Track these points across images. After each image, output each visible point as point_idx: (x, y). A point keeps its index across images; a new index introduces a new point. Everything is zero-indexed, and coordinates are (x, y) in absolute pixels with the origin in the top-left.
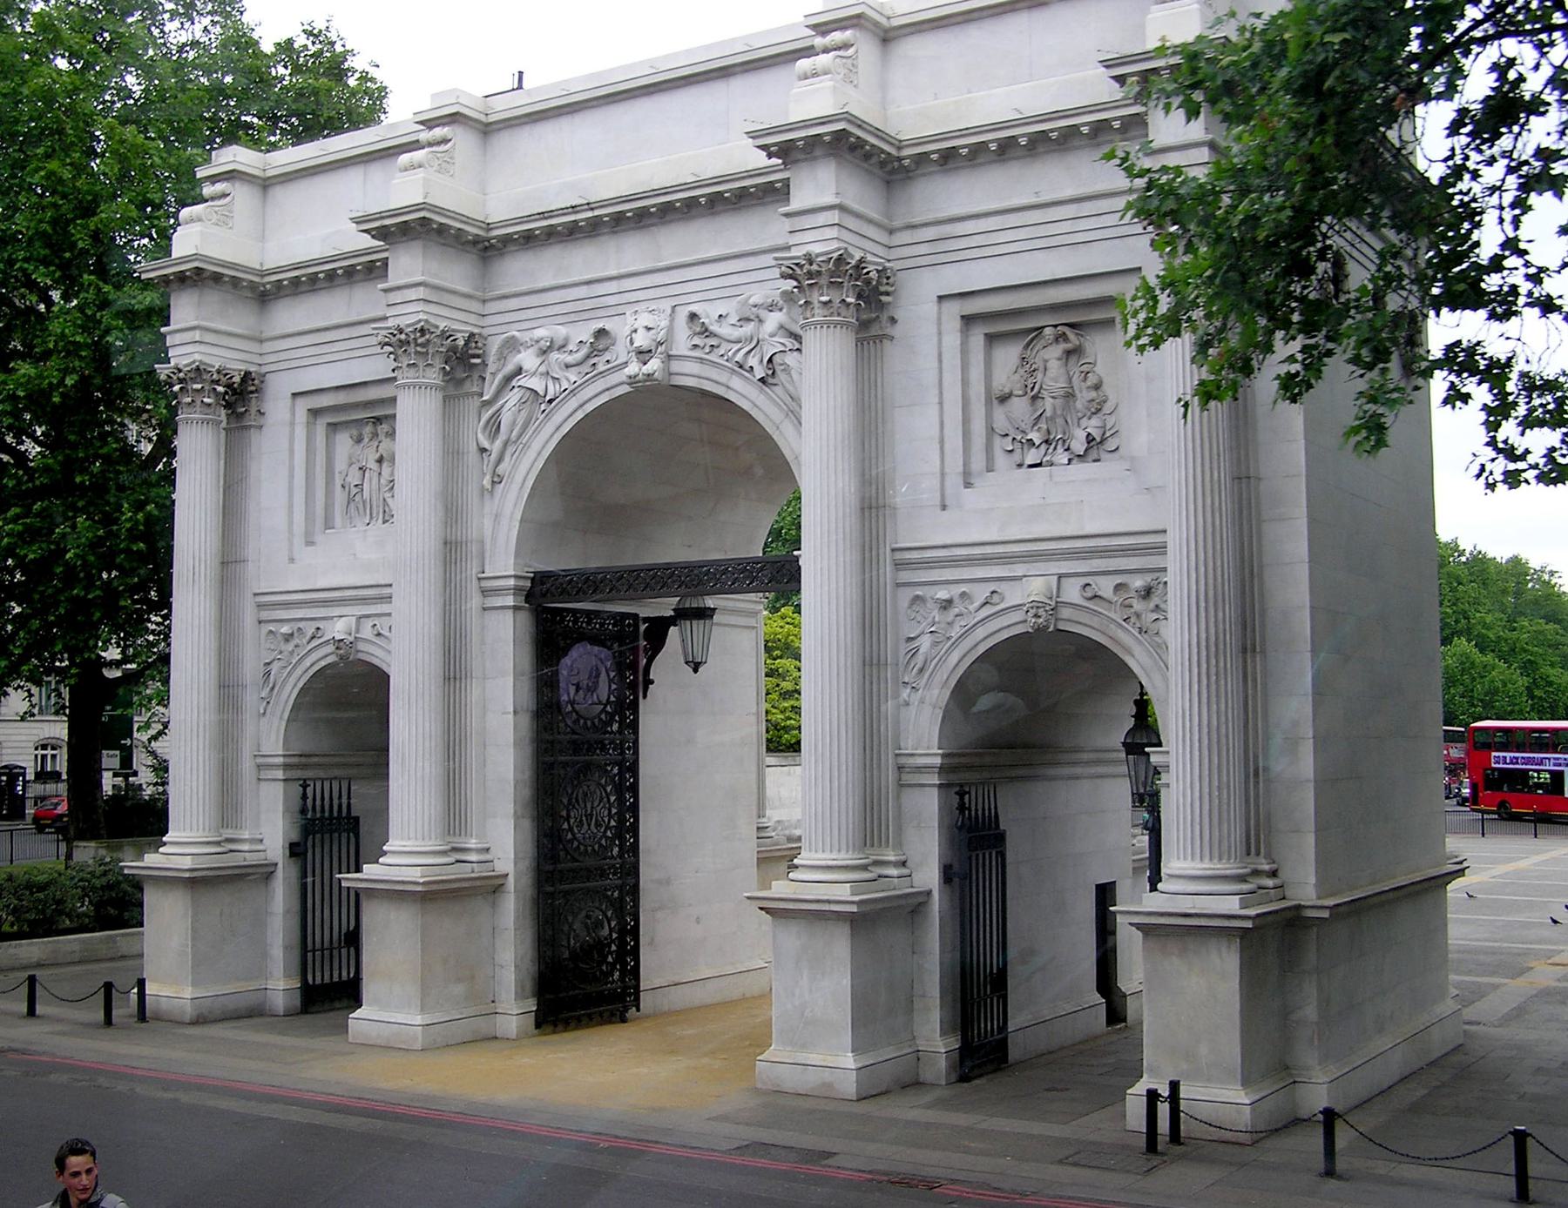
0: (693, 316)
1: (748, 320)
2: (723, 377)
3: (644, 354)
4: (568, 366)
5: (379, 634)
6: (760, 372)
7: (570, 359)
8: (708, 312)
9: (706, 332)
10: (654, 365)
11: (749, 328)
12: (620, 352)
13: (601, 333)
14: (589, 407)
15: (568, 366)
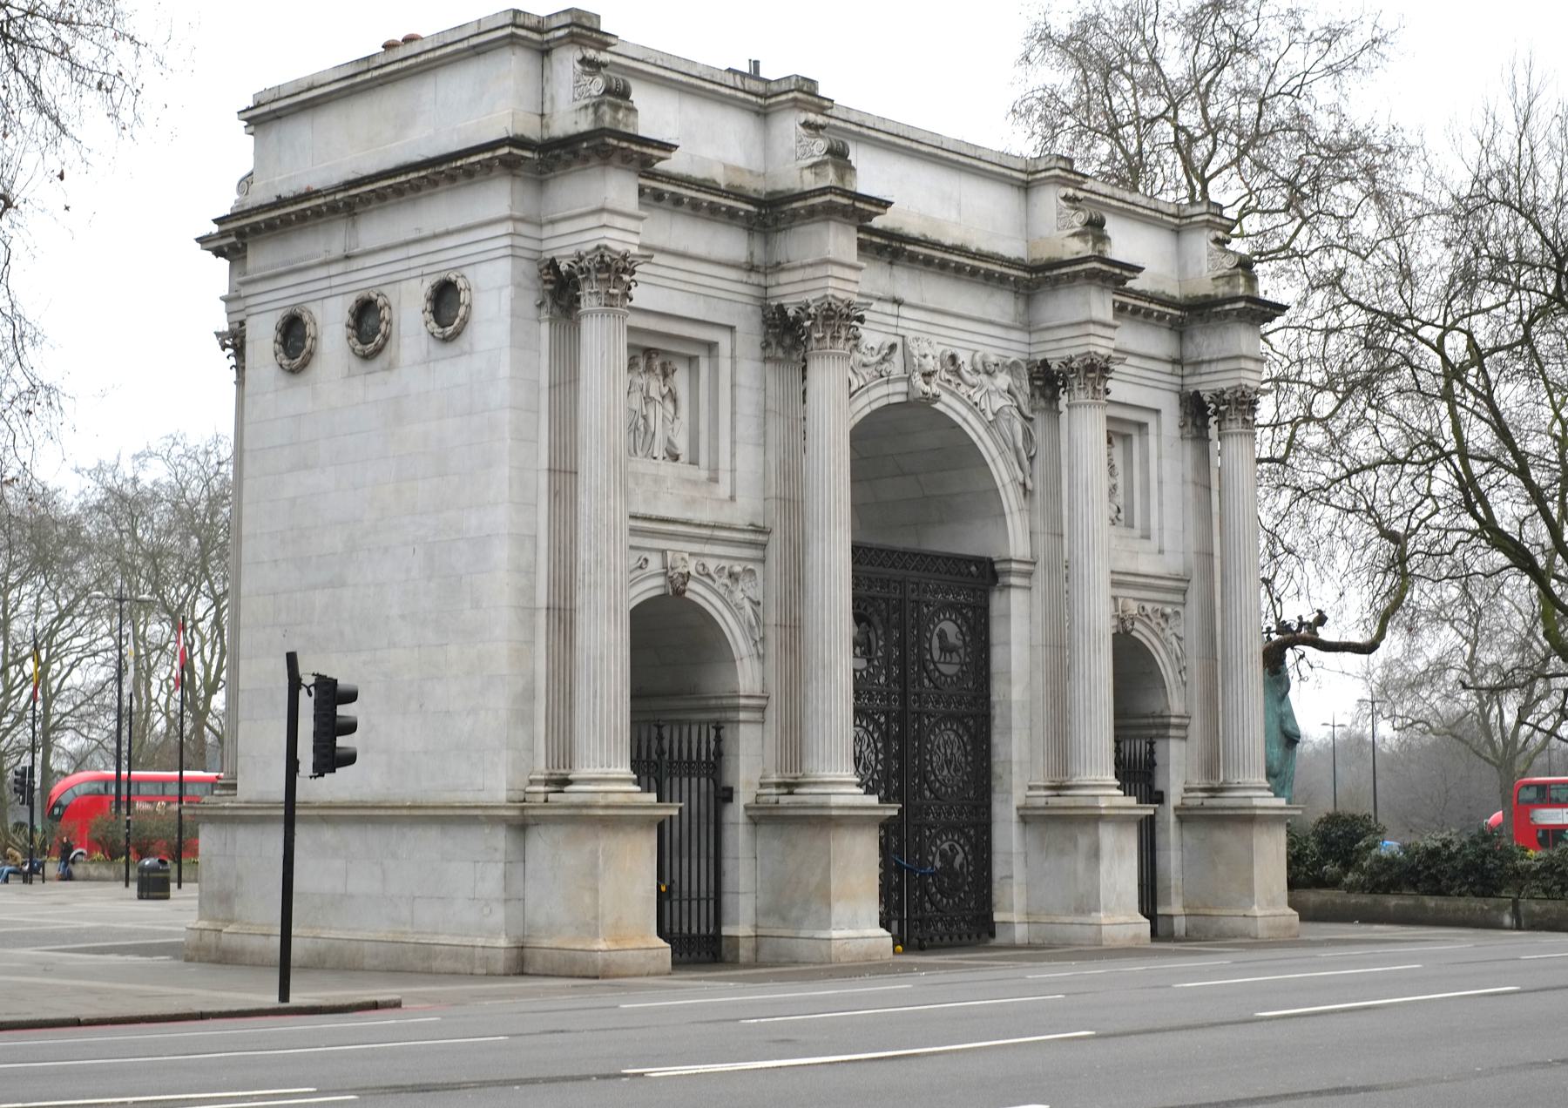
0: (953, 358)
1: (977, 372)
2: (964, 411)
3: (927, 375)
4: (865, 365)
5: (708, 575)
6: (991, 417)
7: (865, 360)
8: (964, 357)
9: (957, 373)
10: (935, 389)
11: (984, 377)
12: (896, 366)
13: (893, 347)
14: (875, 406)
15: (865, 365)
